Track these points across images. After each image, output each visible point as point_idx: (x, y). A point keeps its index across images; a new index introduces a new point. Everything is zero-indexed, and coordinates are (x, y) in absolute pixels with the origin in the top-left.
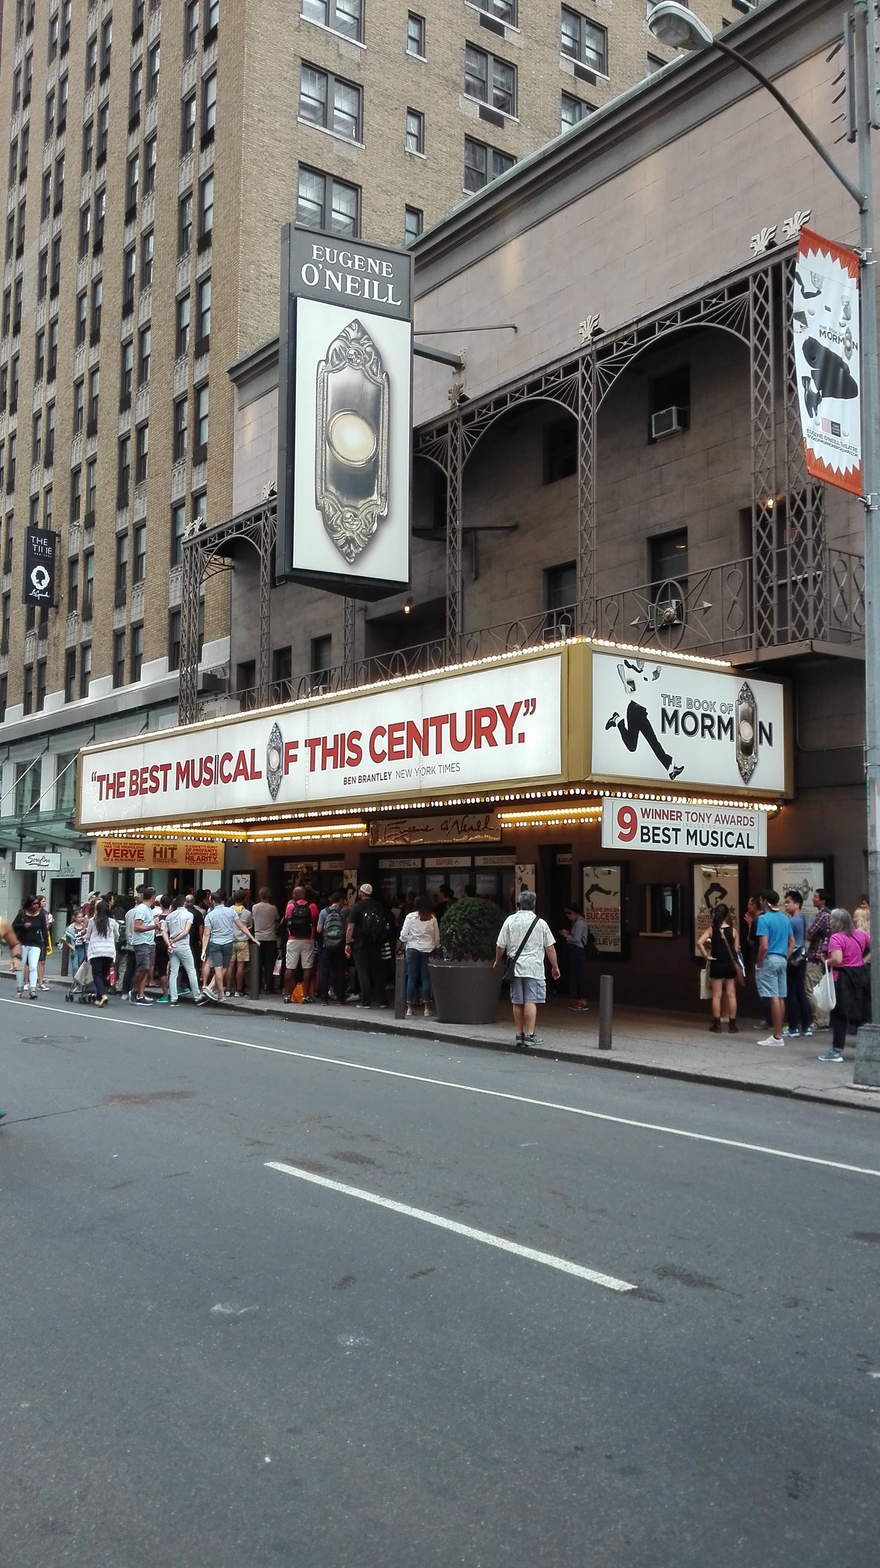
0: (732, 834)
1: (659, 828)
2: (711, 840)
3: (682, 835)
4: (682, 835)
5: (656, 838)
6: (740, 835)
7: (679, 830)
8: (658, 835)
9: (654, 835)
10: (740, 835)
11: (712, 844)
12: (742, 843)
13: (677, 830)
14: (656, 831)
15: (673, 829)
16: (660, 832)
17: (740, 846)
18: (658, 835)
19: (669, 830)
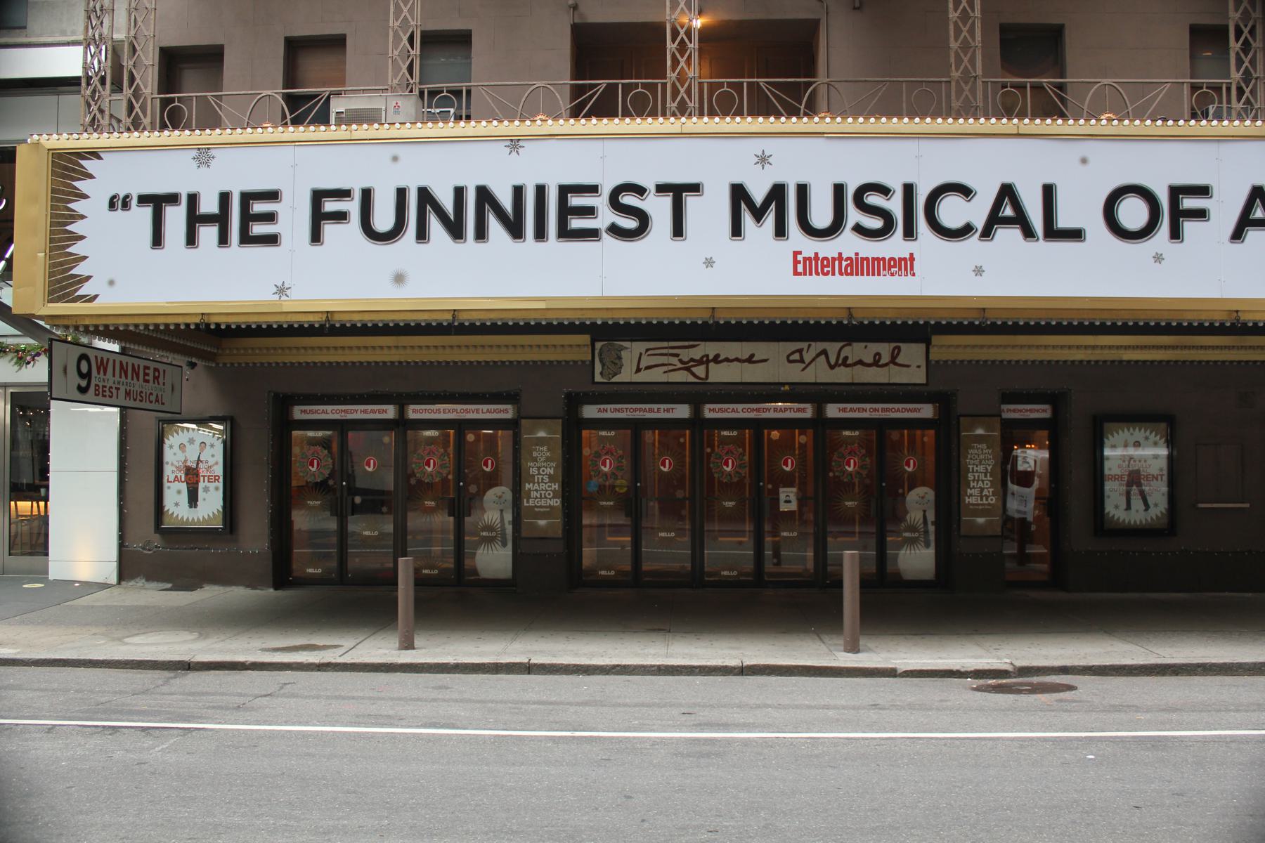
0: (965, 191)
1: (593, 189)
2: (853, 216)
3: (708, 212)
4: (708, 212)
5: (576, 223)
6: (1007, 192)
7: (695, 188)
8: (589, 211)
9: (565, 211)
10: (1007, 192)
11: (858, 229)
12: (1021, 220)
13: (678, 192)
14: (575, 201)
15: (662, 189)
16: (601, 202)
17: (1008, 236)
18: (589, 211)
19: (640, 190)
